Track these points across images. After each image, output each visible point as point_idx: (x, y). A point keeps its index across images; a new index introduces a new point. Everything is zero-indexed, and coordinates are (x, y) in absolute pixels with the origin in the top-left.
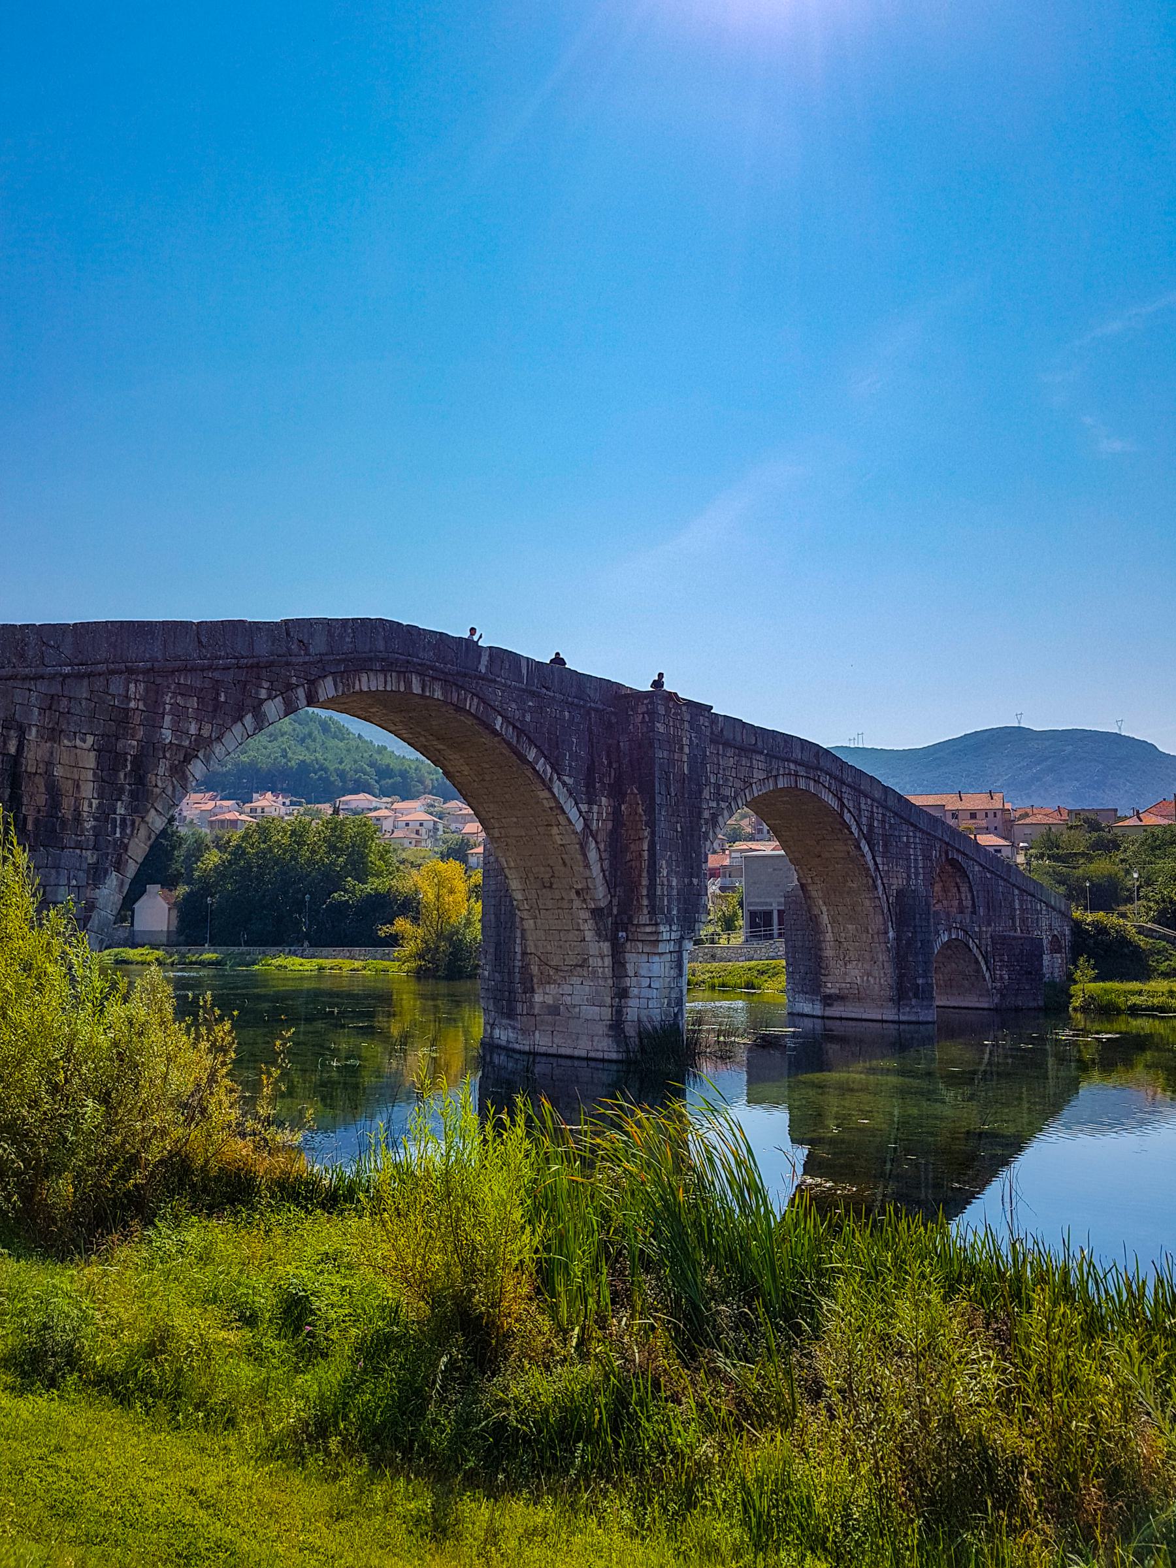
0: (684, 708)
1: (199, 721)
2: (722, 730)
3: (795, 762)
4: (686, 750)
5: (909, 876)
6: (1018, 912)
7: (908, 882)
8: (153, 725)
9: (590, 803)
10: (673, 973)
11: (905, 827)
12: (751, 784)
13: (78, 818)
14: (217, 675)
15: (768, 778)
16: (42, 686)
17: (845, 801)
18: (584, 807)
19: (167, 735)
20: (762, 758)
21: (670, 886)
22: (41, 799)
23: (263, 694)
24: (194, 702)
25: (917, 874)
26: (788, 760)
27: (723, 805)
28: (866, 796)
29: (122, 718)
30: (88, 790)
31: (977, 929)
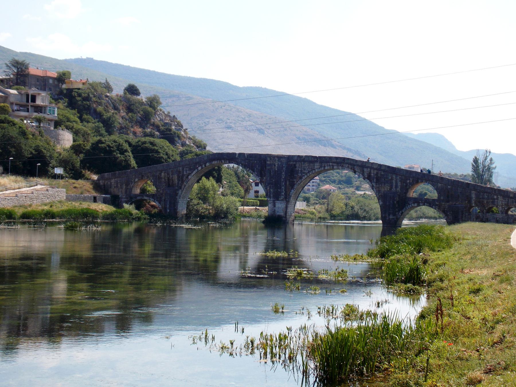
0: (276, 158)
1: (189, 171)
2: (304, 159)
3: (332, 163)
4: (277, 166)
5: (391, 187)
6: (474, 199)
7: (390, 189)
8: (183, 172)
9: (261, 177)
10: (273, 206)
11: (390, 175)
12: (315, 169)
13: (175, 184)
14: (191, 165)
15: (321, 167)
16: (171, 170)
17: (356, 170)
18: (260, 178)
19: (185, 173)
20: (318, 163)
21: (270, 191)
22: (172, 182)
23: (198, 166)
24: (188, 169)
25: (396, 187)
26: (329, 163)
27: (304, 174)
28: (367, 167)
29: (180, 172)
30: (176, 180)
31: (437, 203)
